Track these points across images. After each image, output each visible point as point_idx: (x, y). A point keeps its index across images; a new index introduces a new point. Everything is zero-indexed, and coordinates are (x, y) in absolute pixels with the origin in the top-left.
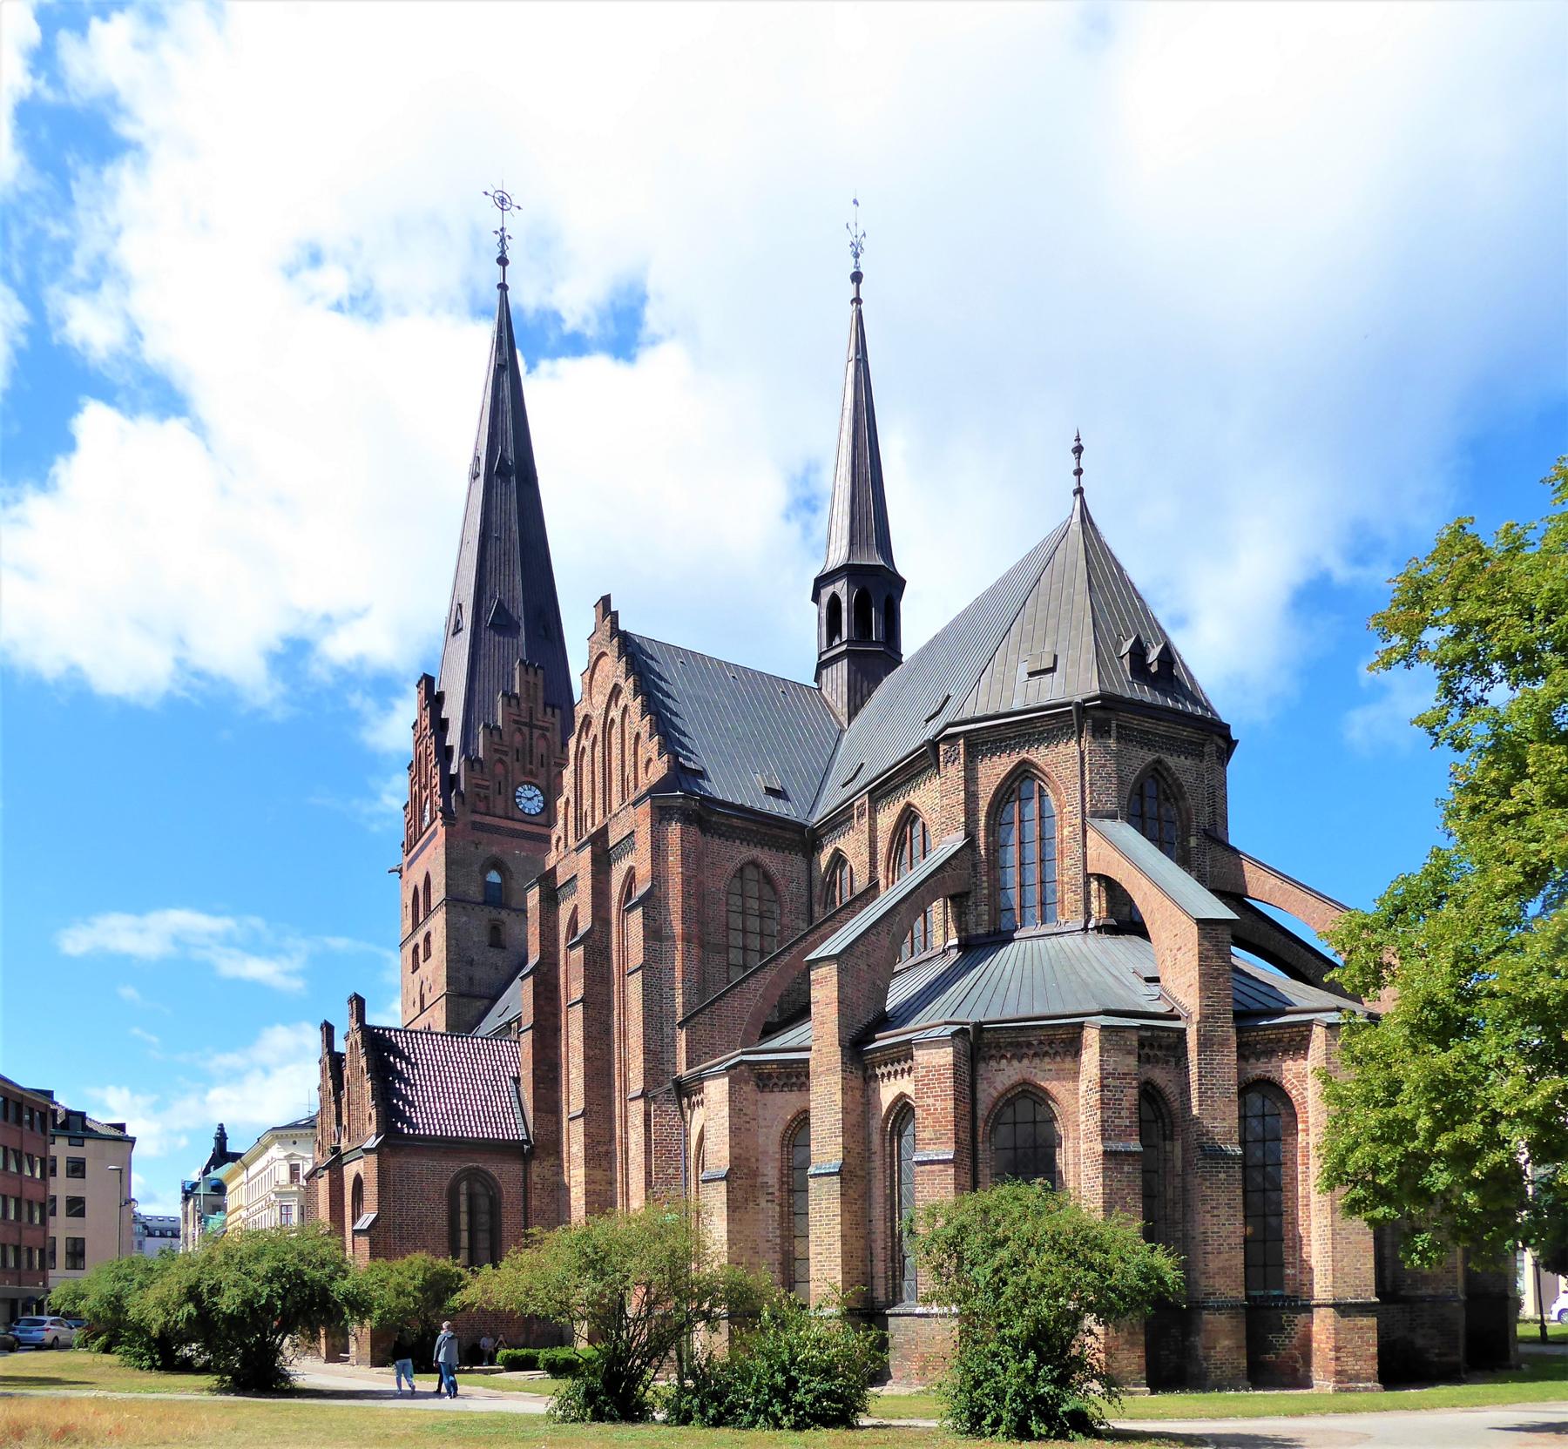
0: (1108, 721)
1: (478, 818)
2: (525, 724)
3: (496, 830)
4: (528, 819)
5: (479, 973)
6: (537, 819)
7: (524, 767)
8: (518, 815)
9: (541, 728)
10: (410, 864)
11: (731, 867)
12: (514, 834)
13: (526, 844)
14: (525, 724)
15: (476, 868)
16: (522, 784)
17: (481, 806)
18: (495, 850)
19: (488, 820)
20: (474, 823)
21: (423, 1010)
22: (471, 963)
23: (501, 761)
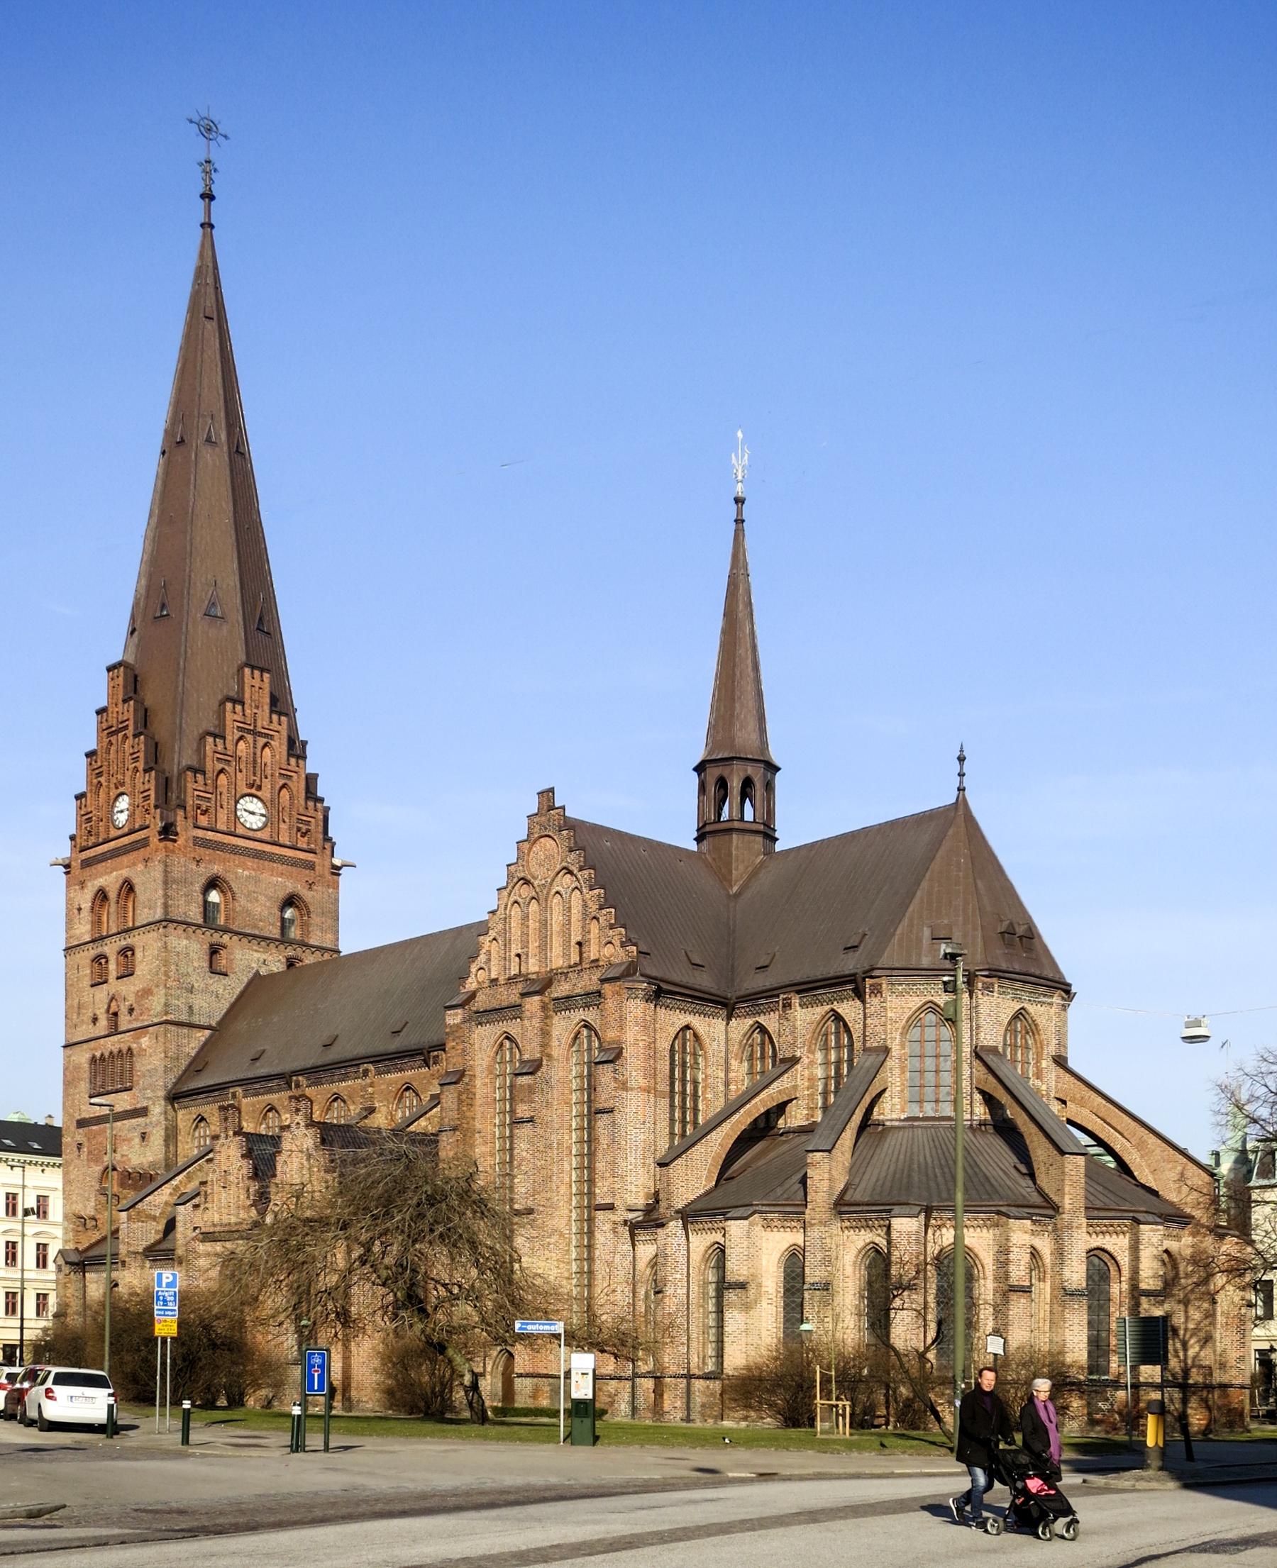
0: (992, 984)
1: (200, 833)
2: (249, 731)
3: (217, 846)
4: (251, 834)
5: (200, 1002)
6: (259, 835)
8: (240, 831)
9: (266, 736)
10: (86, 864)
11: (673, 1031)
12: (235, 850)
13: (250, 862)
14: (249, 731)
15: (198, 887)
16: (243, 796)
17: (203, 821)
18: (217, 869)
20: (195, 838)
21: (114, 1030)
22: (191, 990)
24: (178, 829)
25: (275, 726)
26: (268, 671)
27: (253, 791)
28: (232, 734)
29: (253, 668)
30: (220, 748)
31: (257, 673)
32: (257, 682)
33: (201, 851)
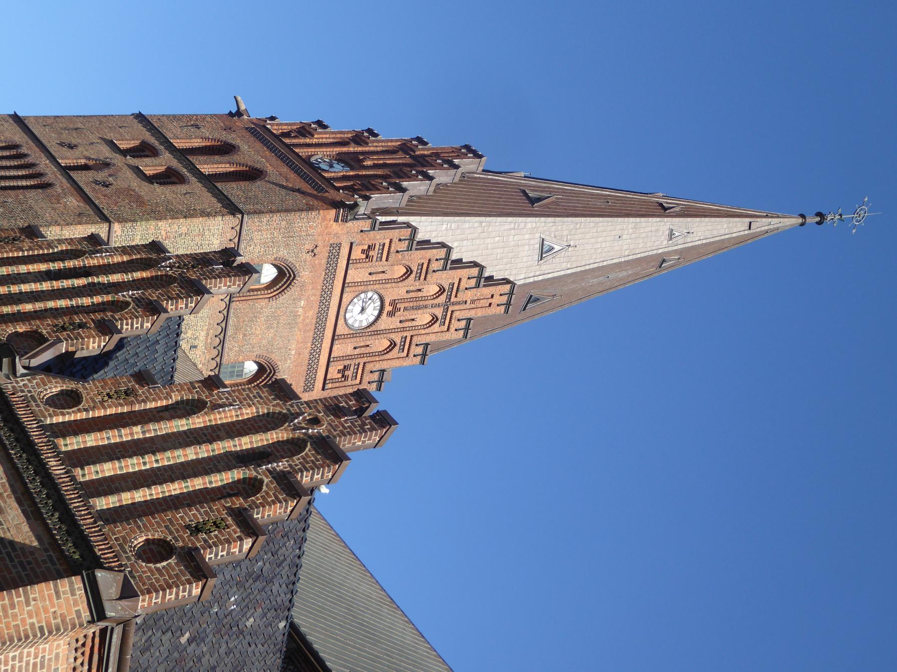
1: (345, 251)
6: (341, 322)
7: (403, 300)
13: (312, 314)
15: (283, 253)
17: (357, 254)
18: (304, 275)
19: (343, 263)
20: (339, 246)
23: (409, 271)
24: (350, 224)
25: (455, 324)
26: (506, 311)
27: (388, 308)
28: (448, 278)
29: (511, 293)
30: (435, 266)
31: (504, 299)
32: (497, 299)
33: (323, 253)
